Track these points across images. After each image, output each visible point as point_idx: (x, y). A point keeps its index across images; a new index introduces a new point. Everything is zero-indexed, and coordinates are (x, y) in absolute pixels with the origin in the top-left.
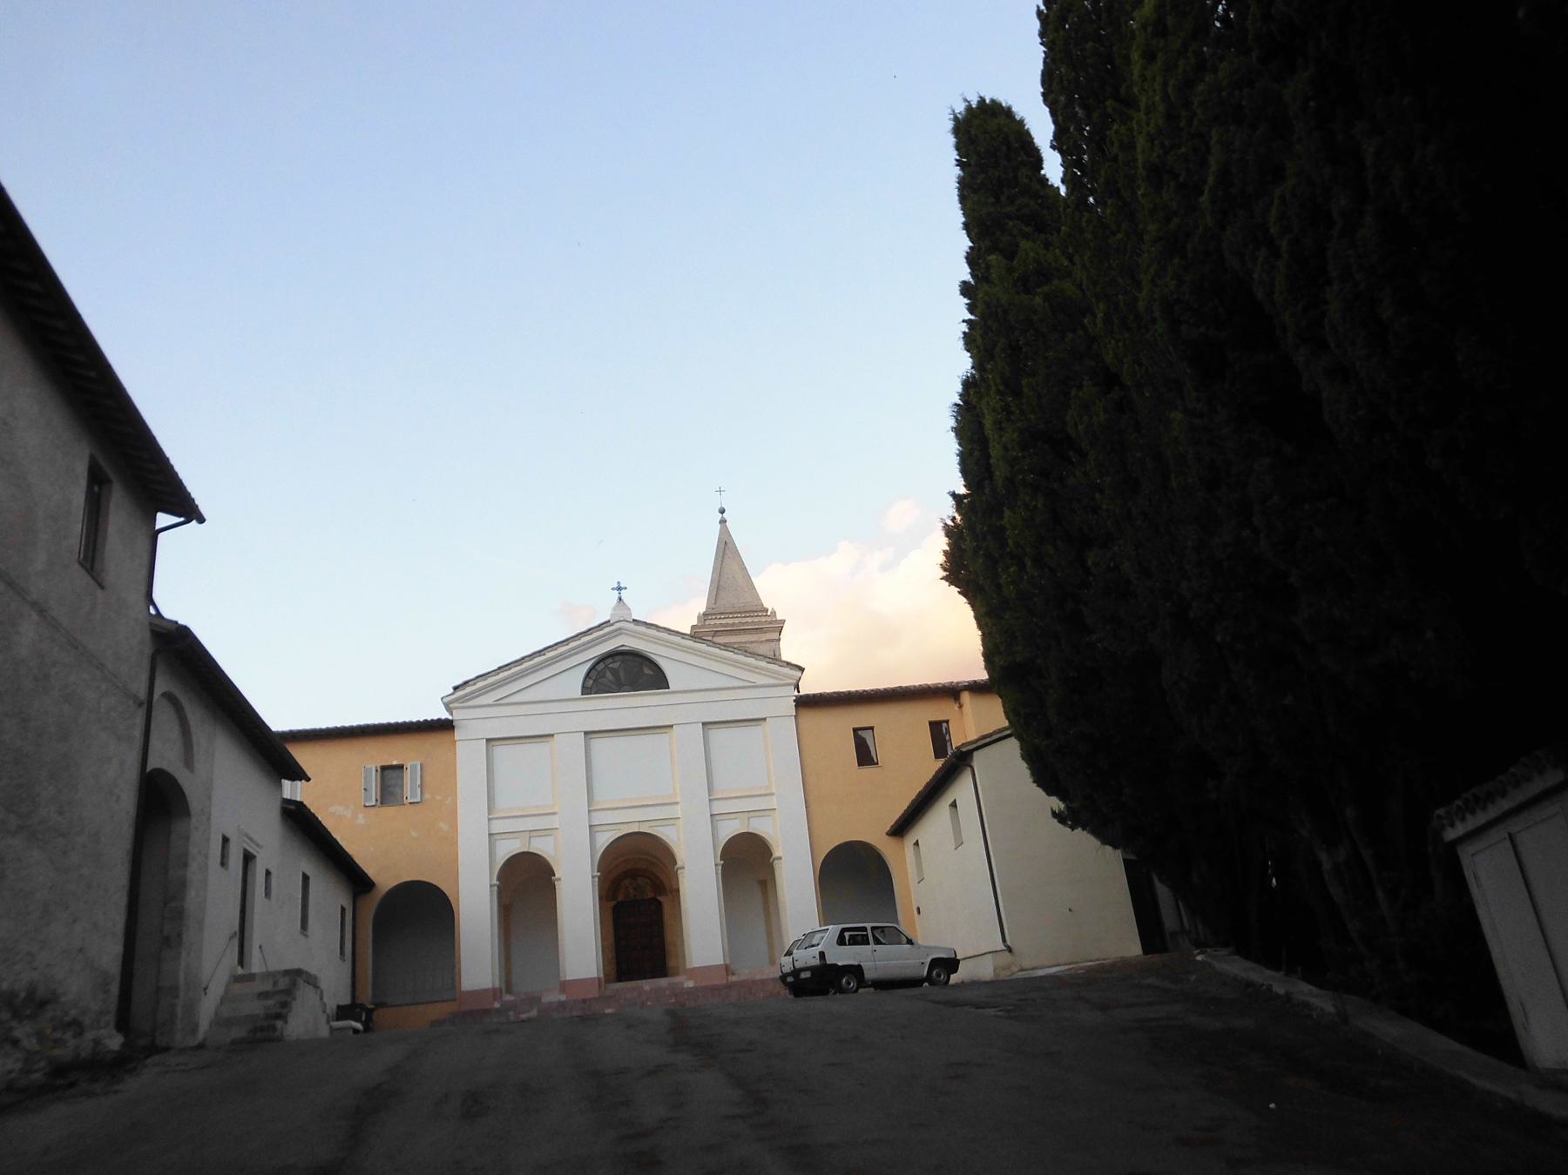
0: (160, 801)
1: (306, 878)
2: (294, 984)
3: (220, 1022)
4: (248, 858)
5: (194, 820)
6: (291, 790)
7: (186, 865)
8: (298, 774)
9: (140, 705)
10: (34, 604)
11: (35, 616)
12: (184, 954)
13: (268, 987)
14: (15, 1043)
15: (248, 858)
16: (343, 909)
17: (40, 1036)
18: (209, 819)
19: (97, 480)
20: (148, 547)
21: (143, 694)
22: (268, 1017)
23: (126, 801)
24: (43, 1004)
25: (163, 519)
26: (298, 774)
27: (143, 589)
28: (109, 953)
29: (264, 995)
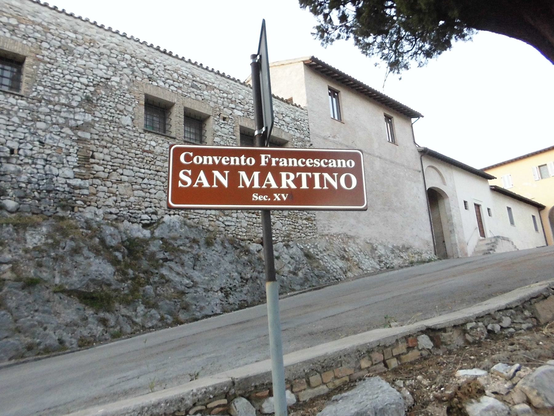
0: (434, 197)
1: (509, 209)
2: (497, 240)
3: (475, 252)
4: (477, 206)
5: (450, 198)
6: (491, 182)
7: (450, 211)
8: (491, 178)
9: (420, 172)
10: (377, 157)
11: (378, 159)
12: (456, 235)
13: (489, 242)
14: (402, 257)
15: (477, 206)
16: (533, 217)
17: (409, 256)
18: (457, 197)
19: (388, 119)
20: (410, 130)
21: (420, 169)
22: (488, 250)
23: (423, 198)
24: (408, 249)
25: (413, 120)
26: (491, 178)
27: (412, 141)
28: (427, 235)
29: (487, 244)
